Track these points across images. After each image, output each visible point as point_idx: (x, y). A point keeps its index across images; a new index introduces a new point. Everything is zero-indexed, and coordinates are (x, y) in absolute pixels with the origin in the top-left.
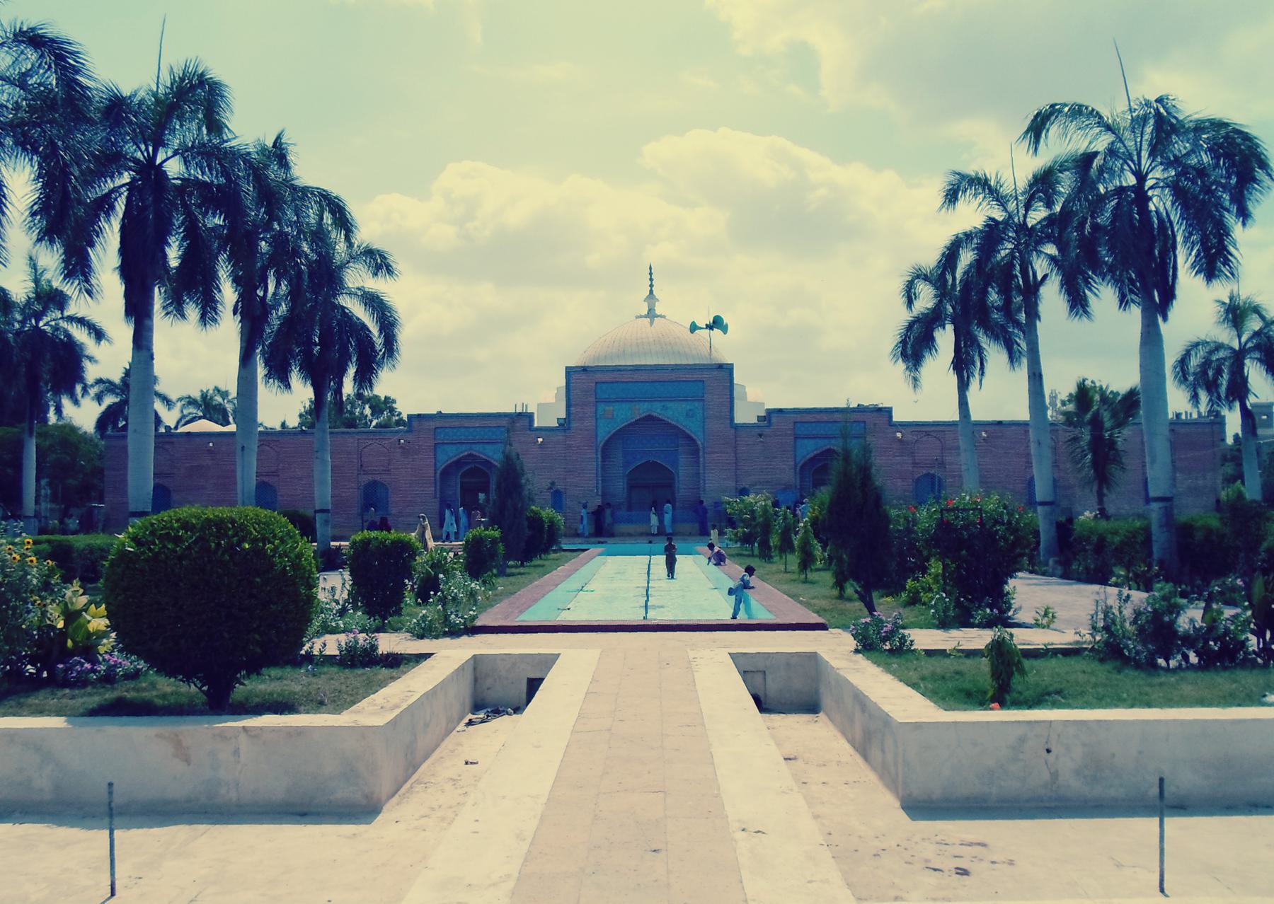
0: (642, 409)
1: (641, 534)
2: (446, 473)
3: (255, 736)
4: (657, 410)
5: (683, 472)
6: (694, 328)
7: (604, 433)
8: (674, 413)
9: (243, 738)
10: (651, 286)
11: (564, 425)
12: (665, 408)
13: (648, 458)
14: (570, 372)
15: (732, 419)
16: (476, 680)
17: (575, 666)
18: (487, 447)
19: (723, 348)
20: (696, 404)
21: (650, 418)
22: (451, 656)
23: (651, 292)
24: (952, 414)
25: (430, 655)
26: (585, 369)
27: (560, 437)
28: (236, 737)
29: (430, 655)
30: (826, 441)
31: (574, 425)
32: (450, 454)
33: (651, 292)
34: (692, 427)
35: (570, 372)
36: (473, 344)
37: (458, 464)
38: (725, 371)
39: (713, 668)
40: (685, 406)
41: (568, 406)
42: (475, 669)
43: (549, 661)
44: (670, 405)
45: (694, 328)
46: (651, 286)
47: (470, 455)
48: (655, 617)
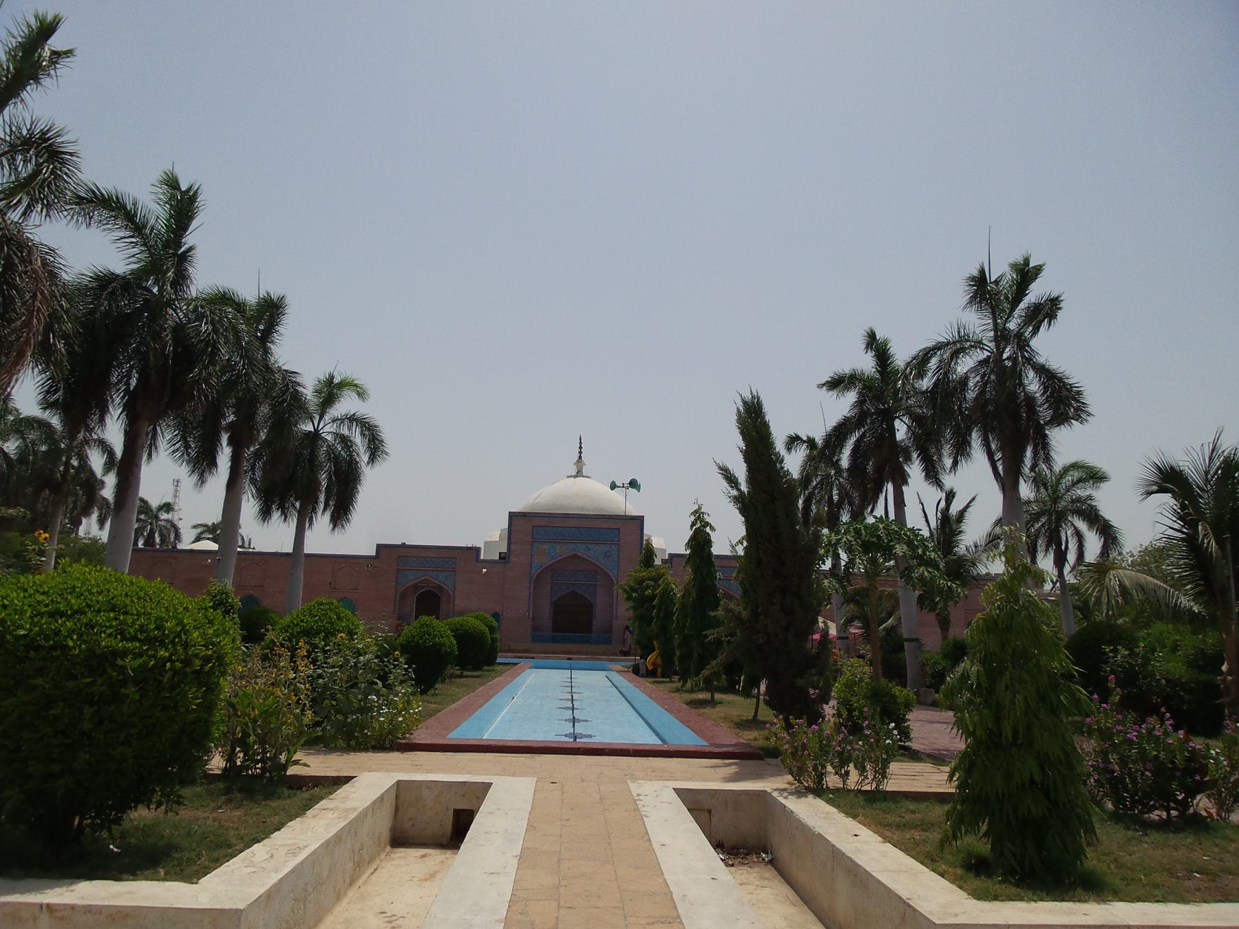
2: (404, 595)
3: (62, 918)
4: (581, 550)
8: (595, 553)
9: (44, 919)
13: (574, 588)
14: (513, 516)
16: (397, 810)
17: (510, 802)
22: (372, 779)
25: (348, 779)
28: (35, 919)
29: (351, 778)
35: (513, 516)
36: (437, 488)
37: (416, 587)
38: (639, 521)
39: (660, 807)
42: (397, 797)
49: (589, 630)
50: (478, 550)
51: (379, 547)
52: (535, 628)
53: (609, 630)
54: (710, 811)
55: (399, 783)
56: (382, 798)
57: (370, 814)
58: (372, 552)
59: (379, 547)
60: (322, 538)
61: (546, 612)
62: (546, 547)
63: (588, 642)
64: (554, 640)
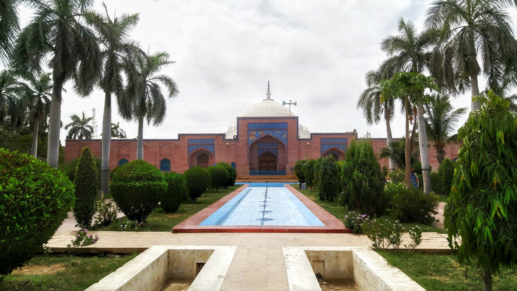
1: (264, 179)
4: (270, 133)
5: (280, 156)
6: (284, 103)
8: (276, 134)
11: (236, 139)
13: (268, 150)
14: (239, 119)
16: (169, 264)
18: (208, 146)
19: (295, 112)
21: (268, 137)
23: (269, 91)
24: (385, 135)
26: (244, 118)
27: (234, 143)
31: (240, 138)
32: (194, 149)
35: (239, 119)
38: (296, 119)
41: (238, 132)
42: (168, 257)
43: (207, 254)
45: (284, 103)
46: (269, 89)
47: (202, 149)
48: (267, 224)
49: (276, 169)
50: (224, 135)
51: (179, 135)
52: (251, 169)
53: (284, 168)
54: (324, 261)
55: (169, 251)
56: (158, 260)
57: (150, 269)
58: (177, 138)
59: (179, 135)
60: (152, 132)
61: (256, 161)
62: (255, 133)
63: (275, 174)
64: (260, 174)
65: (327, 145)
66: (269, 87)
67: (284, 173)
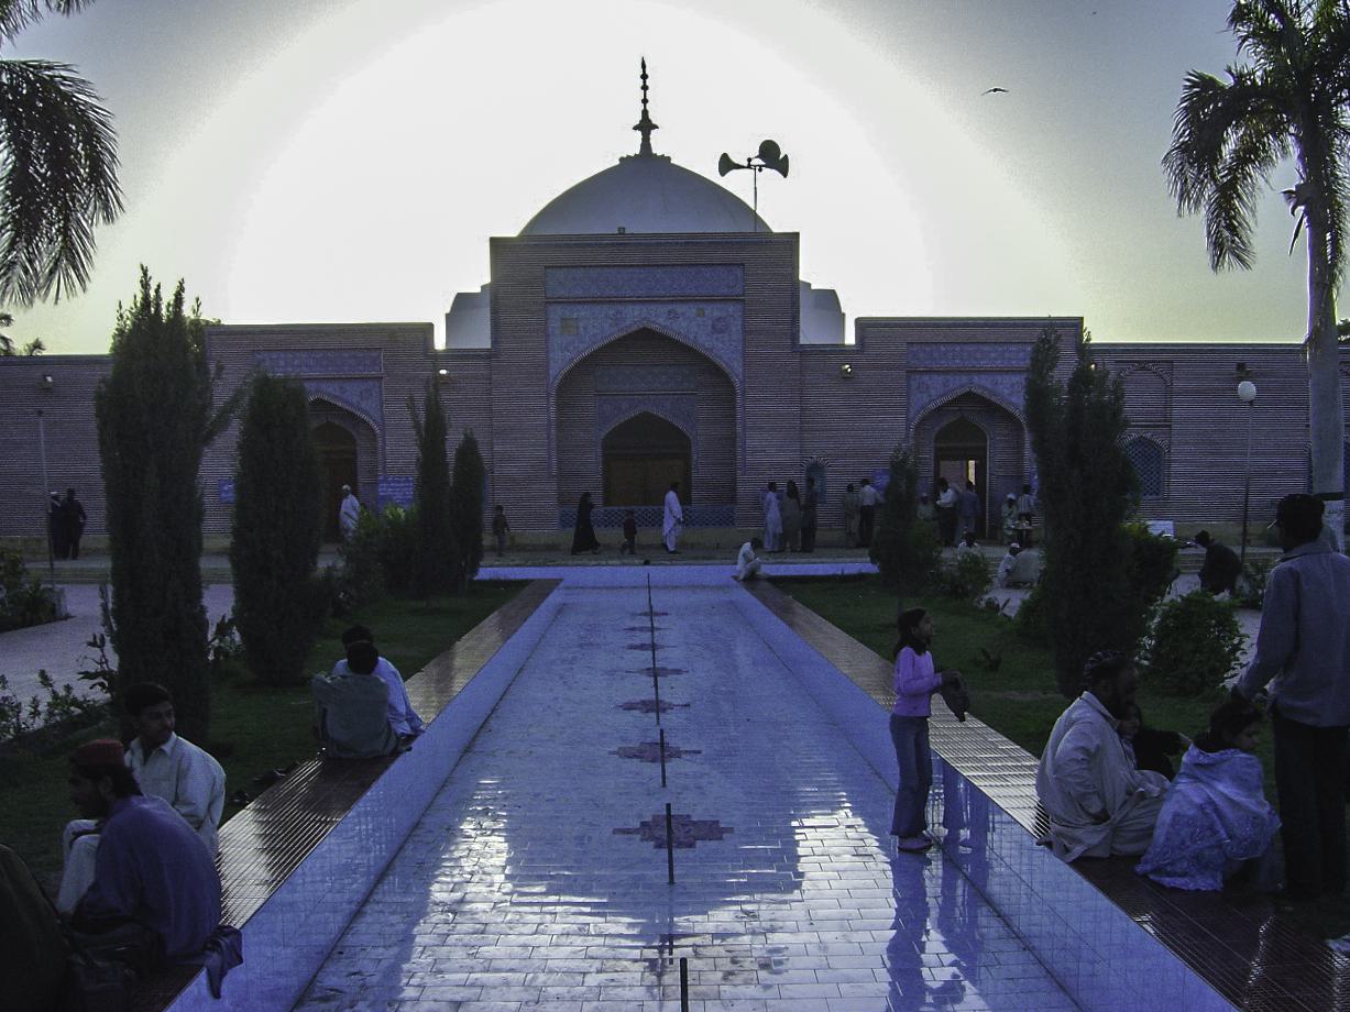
0: (634, 317)
4: (659, 318)
6: (726, 165)
7: (560, 361)
10: (645, 101)
12: (673, 315)
15: (795, 336)
20: (731, 308)
21: (645, 338)
23: (645, 112)
30: (964, 379)
33: (645, 112)
34: (725, 351)
40: (713, 311)
44: (680, 308)
45: (726, 165)
46: (645, 101)
65: (940, 379)
66: (645, 88)
67: (727, 521)
